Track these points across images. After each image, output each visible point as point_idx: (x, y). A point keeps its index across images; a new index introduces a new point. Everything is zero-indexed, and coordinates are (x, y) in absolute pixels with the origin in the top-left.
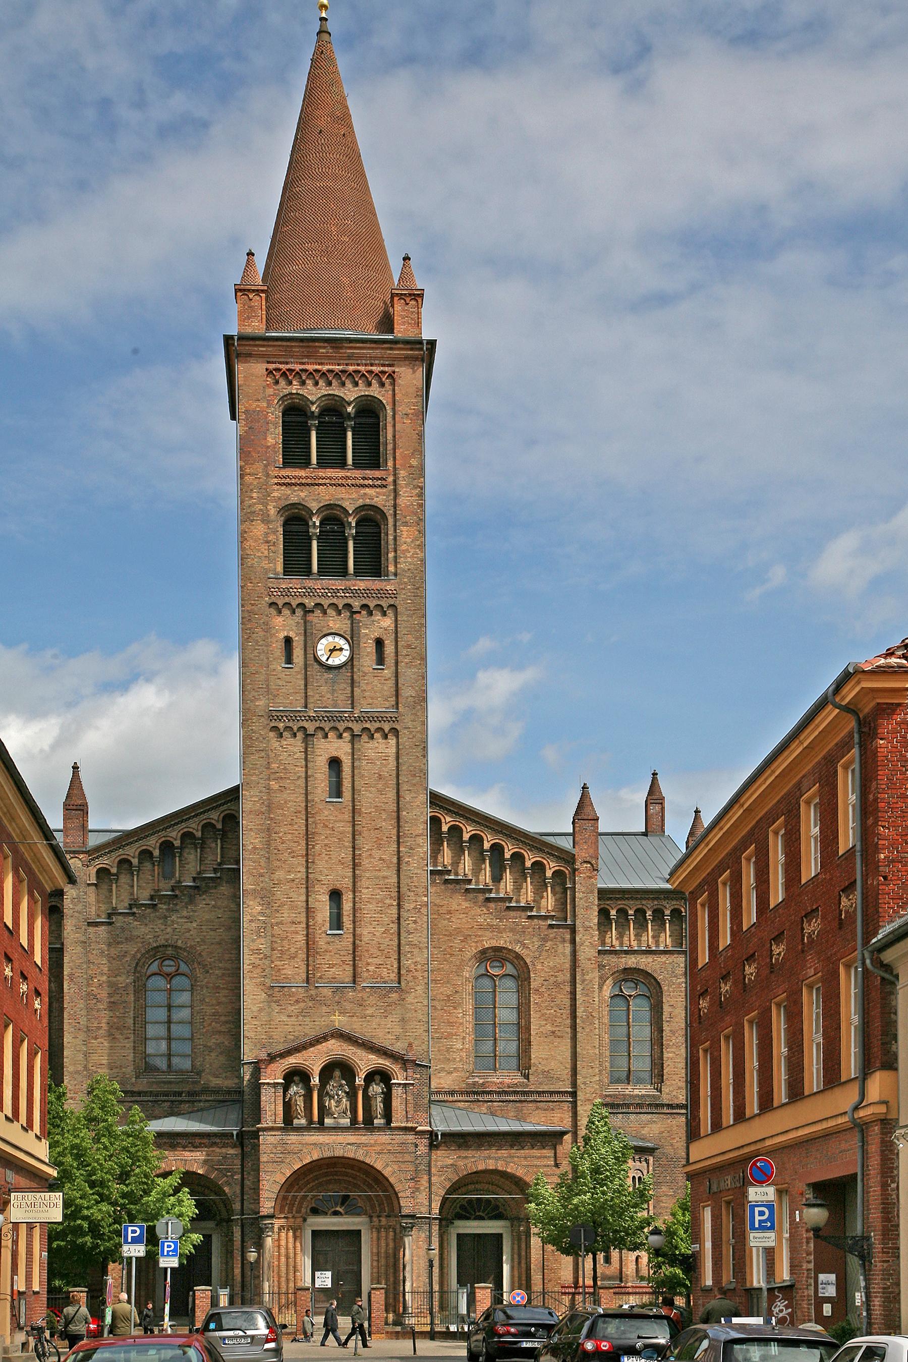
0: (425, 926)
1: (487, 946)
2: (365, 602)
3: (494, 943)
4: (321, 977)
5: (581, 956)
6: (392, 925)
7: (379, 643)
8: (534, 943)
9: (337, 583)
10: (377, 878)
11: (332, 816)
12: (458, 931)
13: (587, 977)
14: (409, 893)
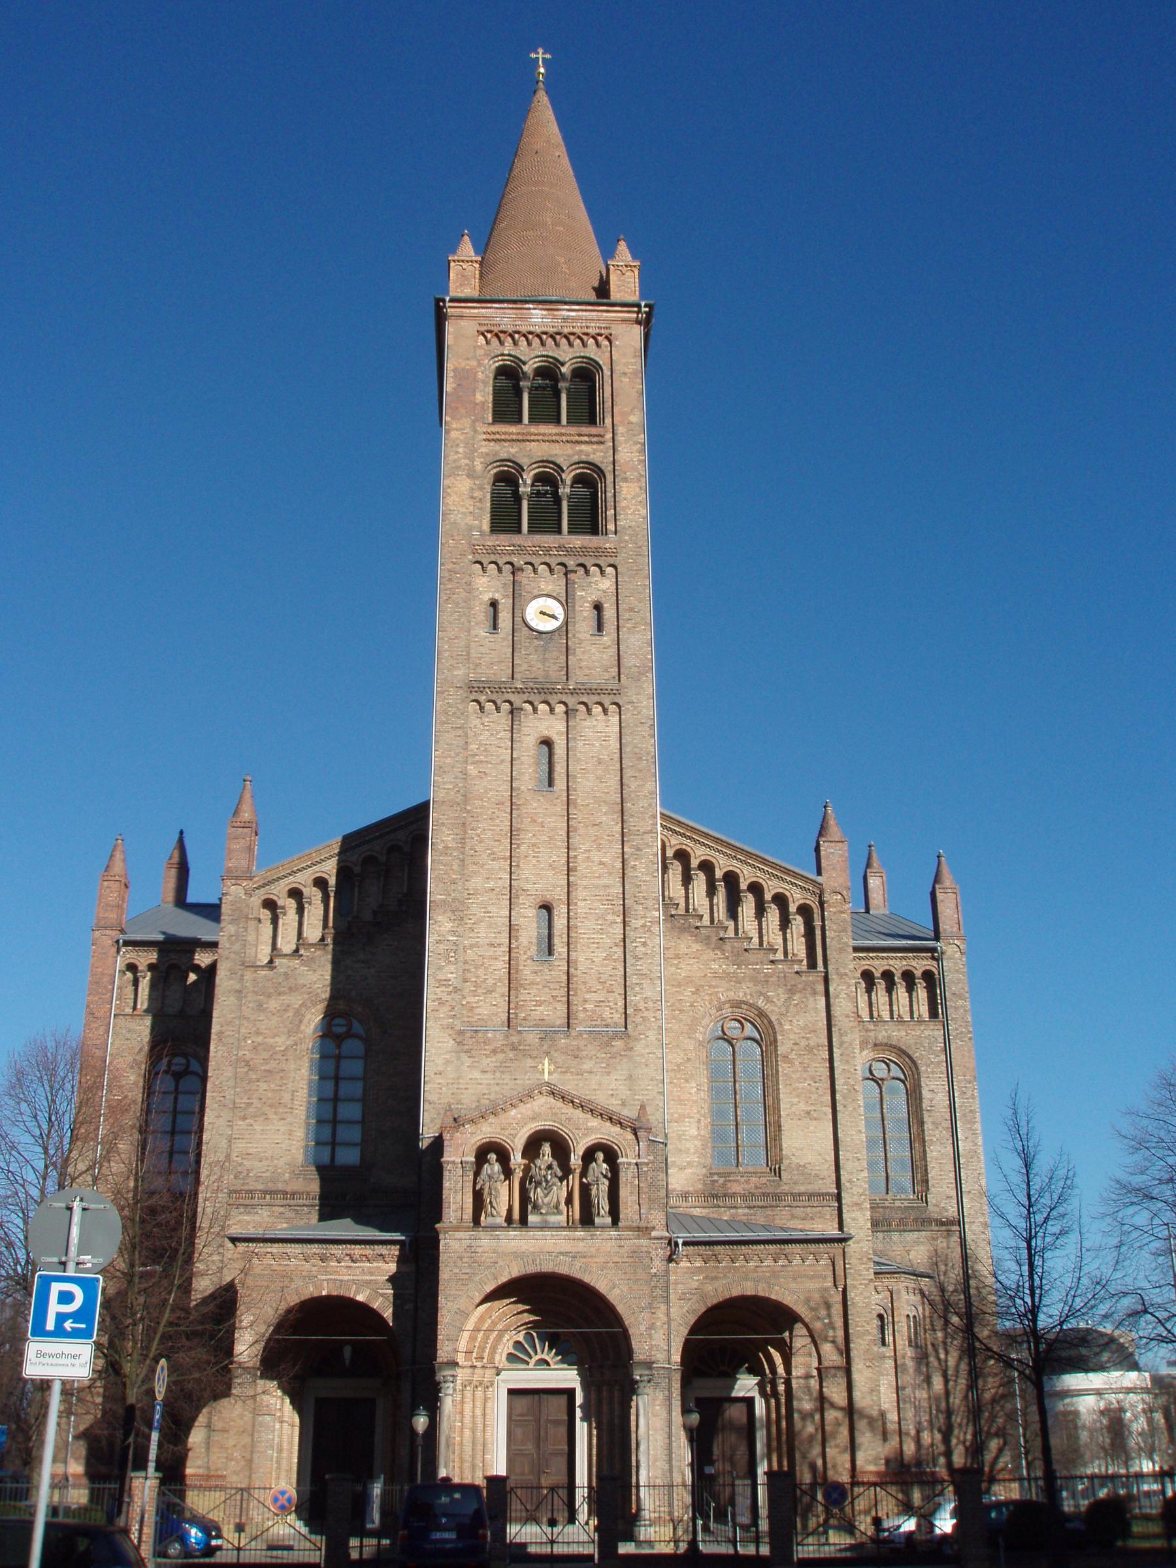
0: (657, 949)
1: (723, 999)
2: (581, 560)
3: (731, 995)
4: (525, 1019)
5: (836, 1011)
6: (615, 949)
7: (598, 607)
8: (778, 995)
9: (549, 540)
10: (596, 887)
11: (544, 812)
12: (689, 981)
13: (845, 1039)
14: (636, 907)
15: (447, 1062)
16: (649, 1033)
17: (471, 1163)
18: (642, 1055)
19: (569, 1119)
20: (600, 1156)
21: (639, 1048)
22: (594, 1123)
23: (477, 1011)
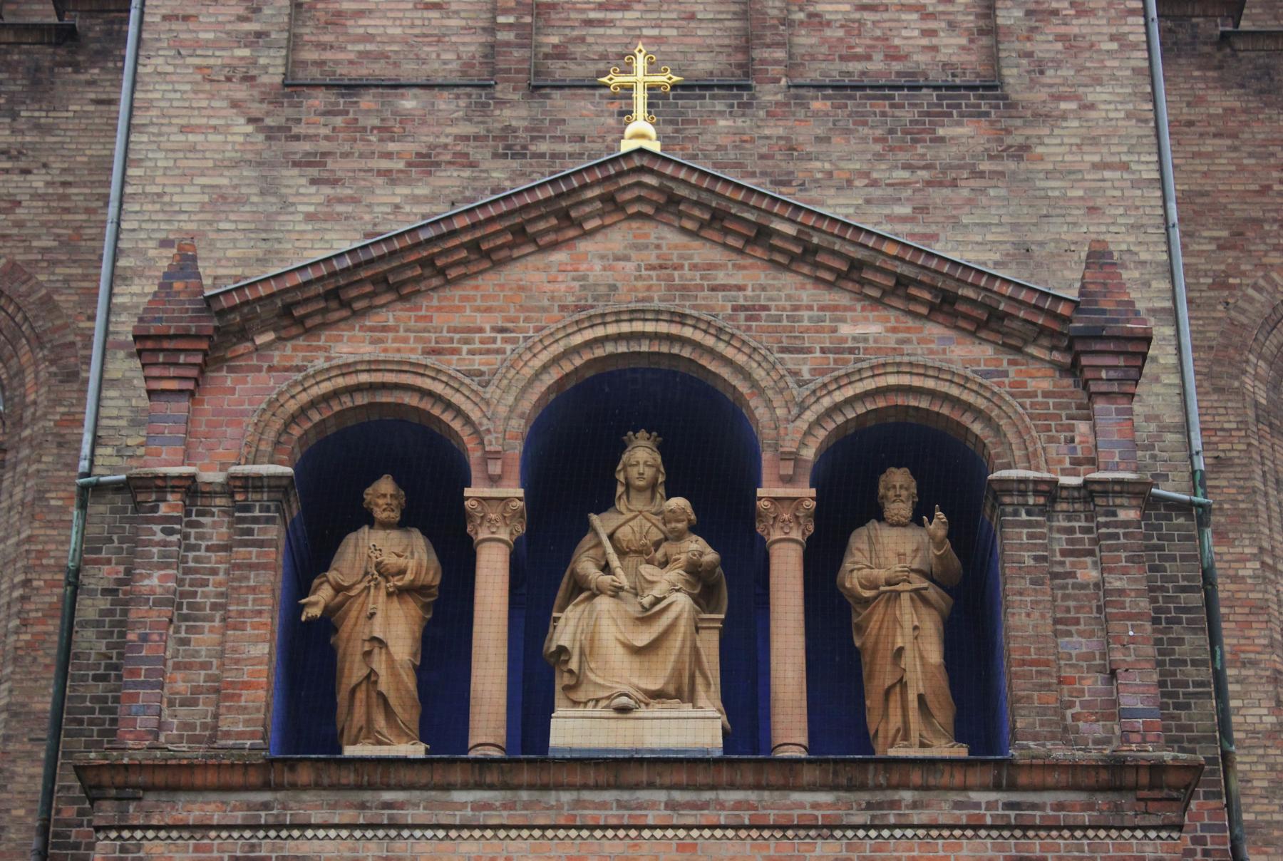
4: (560, 54)
15: (220, 200)
16: (1095, 94)
17: (273, 484)
18: (1068, 173)
19: (752, 311)
20: (898, 486)
21: (1055, 146)
22: (867, 327)
23: (357, 27)
